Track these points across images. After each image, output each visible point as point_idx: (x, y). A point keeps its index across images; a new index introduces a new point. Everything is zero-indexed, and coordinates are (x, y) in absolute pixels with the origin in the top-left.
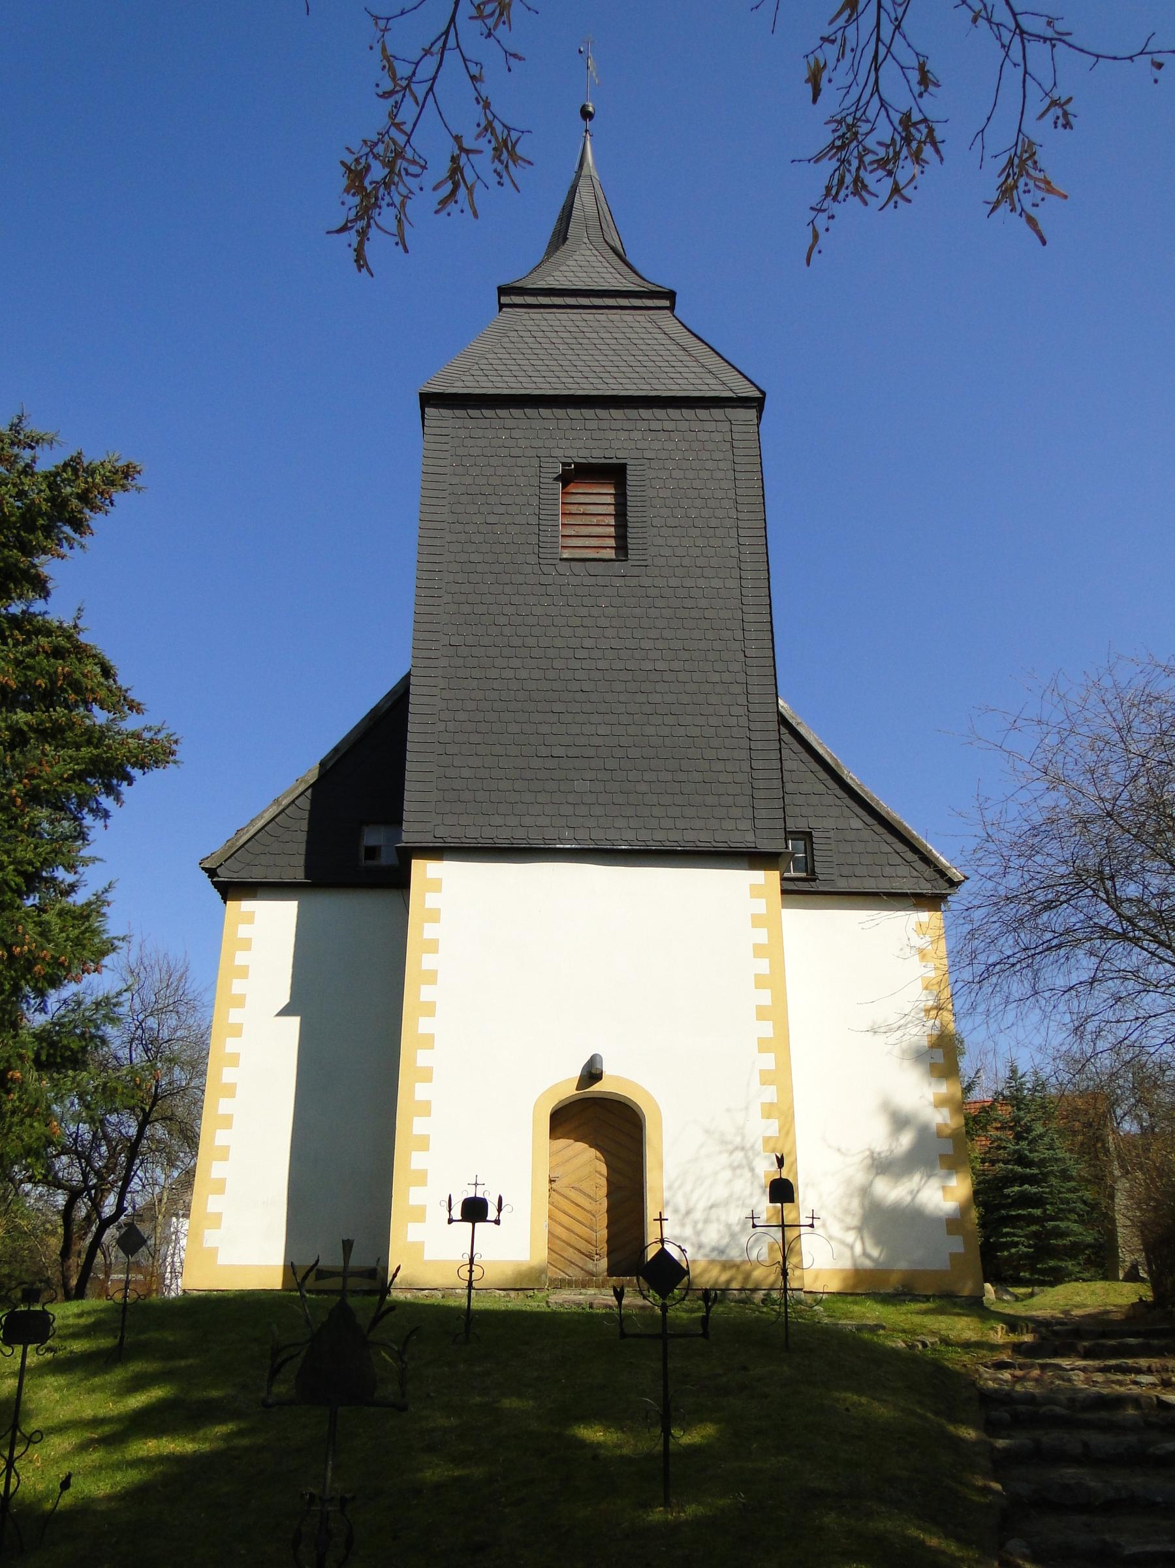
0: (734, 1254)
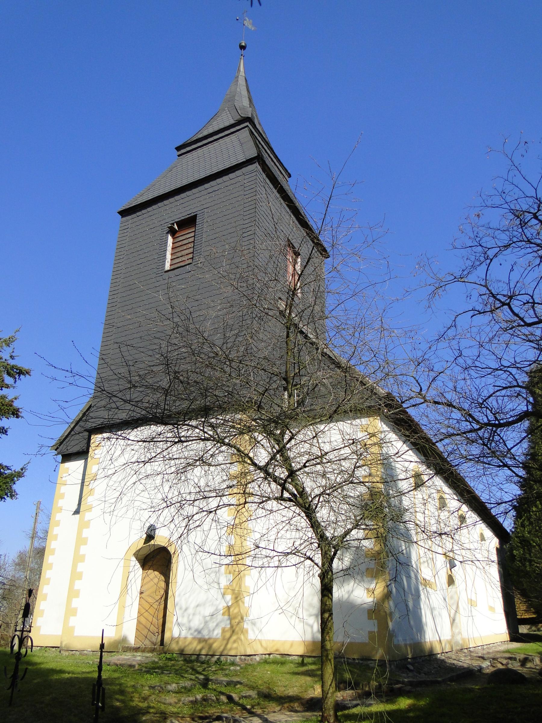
0: (205, 633)
